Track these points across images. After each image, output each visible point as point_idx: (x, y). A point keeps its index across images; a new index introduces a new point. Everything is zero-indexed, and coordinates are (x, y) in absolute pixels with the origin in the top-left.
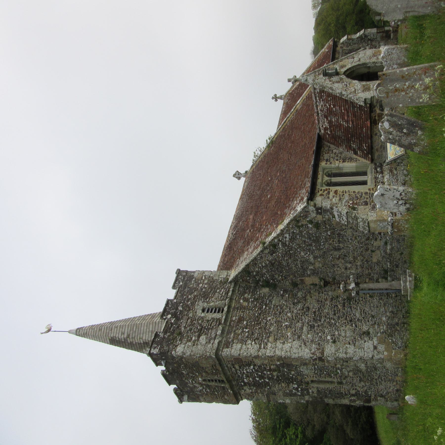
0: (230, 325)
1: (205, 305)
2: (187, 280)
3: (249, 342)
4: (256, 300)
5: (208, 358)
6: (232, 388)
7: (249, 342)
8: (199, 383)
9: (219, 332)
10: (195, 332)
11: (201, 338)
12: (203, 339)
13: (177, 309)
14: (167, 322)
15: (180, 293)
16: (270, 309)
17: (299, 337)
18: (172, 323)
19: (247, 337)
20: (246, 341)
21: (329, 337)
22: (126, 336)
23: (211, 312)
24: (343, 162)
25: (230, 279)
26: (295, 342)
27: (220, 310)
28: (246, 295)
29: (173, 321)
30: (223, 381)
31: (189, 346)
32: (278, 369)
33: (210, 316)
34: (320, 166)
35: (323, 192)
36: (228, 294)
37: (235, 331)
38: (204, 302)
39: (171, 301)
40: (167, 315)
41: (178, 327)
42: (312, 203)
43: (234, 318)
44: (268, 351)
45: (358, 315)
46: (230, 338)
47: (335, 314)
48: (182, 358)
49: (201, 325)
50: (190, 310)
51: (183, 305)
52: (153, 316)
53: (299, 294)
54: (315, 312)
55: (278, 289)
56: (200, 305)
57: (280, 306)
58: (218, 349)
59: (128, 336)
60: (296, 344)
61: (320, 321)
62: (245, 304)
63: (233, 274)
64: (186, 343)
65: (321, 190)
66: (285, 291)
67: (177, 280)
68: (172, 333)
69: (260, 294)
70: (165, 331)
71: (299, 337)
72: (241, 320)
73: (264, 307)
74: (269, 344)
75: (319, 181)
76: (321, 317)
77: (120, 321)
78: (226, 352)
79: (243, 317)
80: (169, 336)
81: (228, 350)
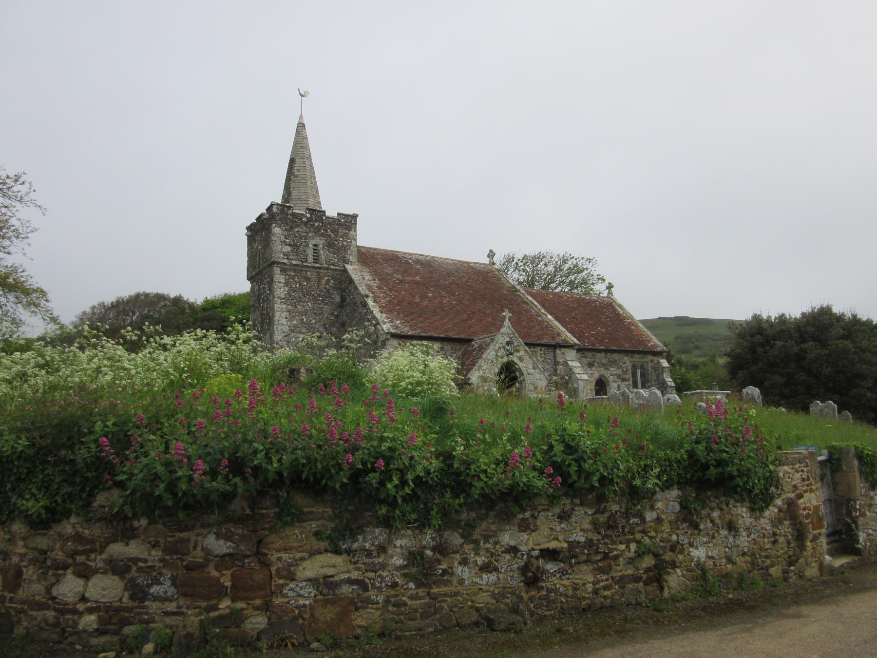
0: (302, 271)
1: (321, 246)
2: (346, 226)
3: (287, 289)
4: (328, 291)
5: (271, 254)
6: (256, 274)
7: (287, 289)
8: (257, 248)
9: (294, 262)
10: (293, 241)
12: (289, 249)
13: (316, 221)
14: (303, 214)
17: (292, 331)
18: (301, 219)
19: (291, 287)
20: (287, 286)
22: (296, 173)
25: (347, 266)
26: (287, 327)
27: (316, 260)
28: (332, 281)
30: (259, 267)
31: (280, 237)
32: (268, 314)
33: (310, 252)
38: (324, 244)
40: (310, 214)
41: (298, 225)
42: (389, 336)
43: (309, 273)
44: (278, 306)
48: (270, 232)
49: (301, 245)
50: (315, 233)
51: (319, 225)
52: (316, 195)
53: (334, 329)
55: (339, 310)
56: (321, 242)
57: (322, 313)
58: (279, 263)
59: (296, 176)
60: (286, 329)
62: (323, 282)
63: (353, 269)
66: (337, 316)
67: (347, 216)
68: (292, 221)
69: (334, 294)
70: (293, 214)
71: (292, 331)
72: (308, 279)
74: (284, 306)
77: (311, 165)
78: (277, 270)
79: (310, 281)
81: (279, 272)
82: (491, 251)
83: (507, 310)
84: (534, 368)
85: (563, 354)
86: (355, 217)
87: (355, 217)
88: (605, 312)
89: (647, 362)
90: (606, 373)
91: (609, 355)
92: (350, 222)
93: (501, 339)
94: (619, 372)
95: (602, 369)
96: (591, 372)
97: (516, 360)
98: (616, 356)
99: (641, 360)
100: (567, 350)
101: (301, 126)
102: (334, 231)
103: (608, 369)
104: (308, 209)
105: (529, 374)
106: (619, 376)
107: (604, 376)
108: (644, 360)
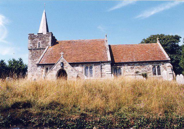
7: (31, 55)
27: (39, 47)
33: (38, 45)
56: (40, 42)
72: (37, 52)
102: (45, 38)
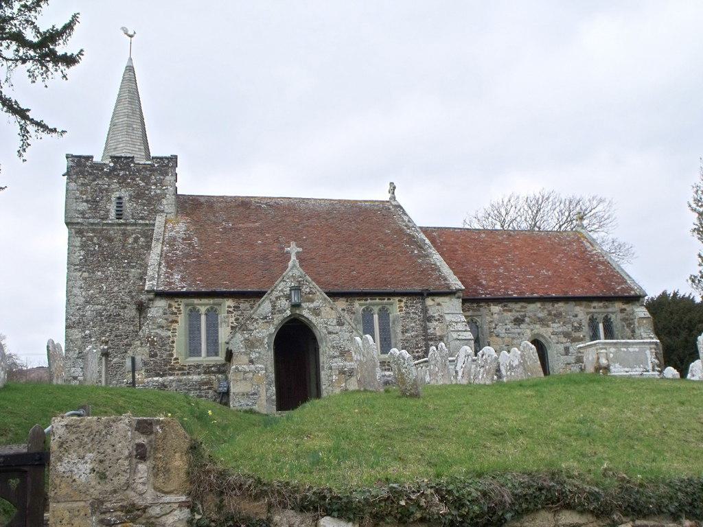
3: (82, 253)
7: (82, 253)
9: (91, 221)
11: (85, 204)
13: (121, 170)
15: (144, 167)
16: (124, 267)
17: (87, 302)
19: (89, 250)
21: (87, 332)
23: (117, 207)
24: (232, 327)
27: (119, 216)
28: (142, 239)
29: (105, 170)
34: (225, 299)
35: (175, 308)
36: (141, 219)
37: (95, 236)
38: (130, 196)
39: (132, 161)
45: (115, 360)
46: (87, 232)
47: (116, 336)
51: (126, 175)
54: (119, 315)
56: (125, 194)
57: (128, 278)
61: (108, 322)
62: (130, 240)
64: (77, 189)
65: (179, 305)
72: (110, 240)
73: (126, 261)
75: (196, 301)
76: (113, 321)
79: (113, 241)
80: (88, 171)
82: (392, 183)
83: (293, 244)
84: (340, 323)
85: (439, 304)
86: (173, 160)
87: (173, 160)
88: (565, 250)
89: (613, 313)
90: (545, 332)
91: (549, 306)
92: (167, 165)
93: (283, 286)
94: (565, 329)
95: (538, 326)
96: (519, 330)
97: (305, 313)
98: (561, 306)
99: (603, 310)
100: (446, 299)
101: (130, 69)
103: (548, 326)
104: (111, 157)
105: (330, 333)
106: (567, 335)
107: (542, 336)
108: (610, 310)
